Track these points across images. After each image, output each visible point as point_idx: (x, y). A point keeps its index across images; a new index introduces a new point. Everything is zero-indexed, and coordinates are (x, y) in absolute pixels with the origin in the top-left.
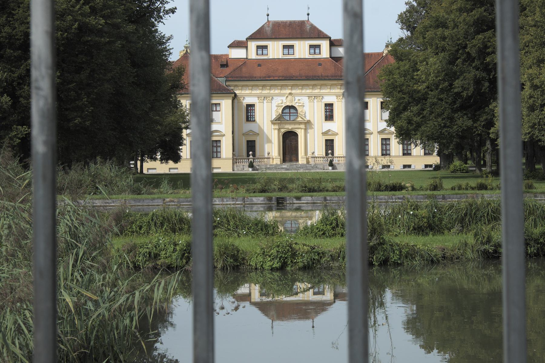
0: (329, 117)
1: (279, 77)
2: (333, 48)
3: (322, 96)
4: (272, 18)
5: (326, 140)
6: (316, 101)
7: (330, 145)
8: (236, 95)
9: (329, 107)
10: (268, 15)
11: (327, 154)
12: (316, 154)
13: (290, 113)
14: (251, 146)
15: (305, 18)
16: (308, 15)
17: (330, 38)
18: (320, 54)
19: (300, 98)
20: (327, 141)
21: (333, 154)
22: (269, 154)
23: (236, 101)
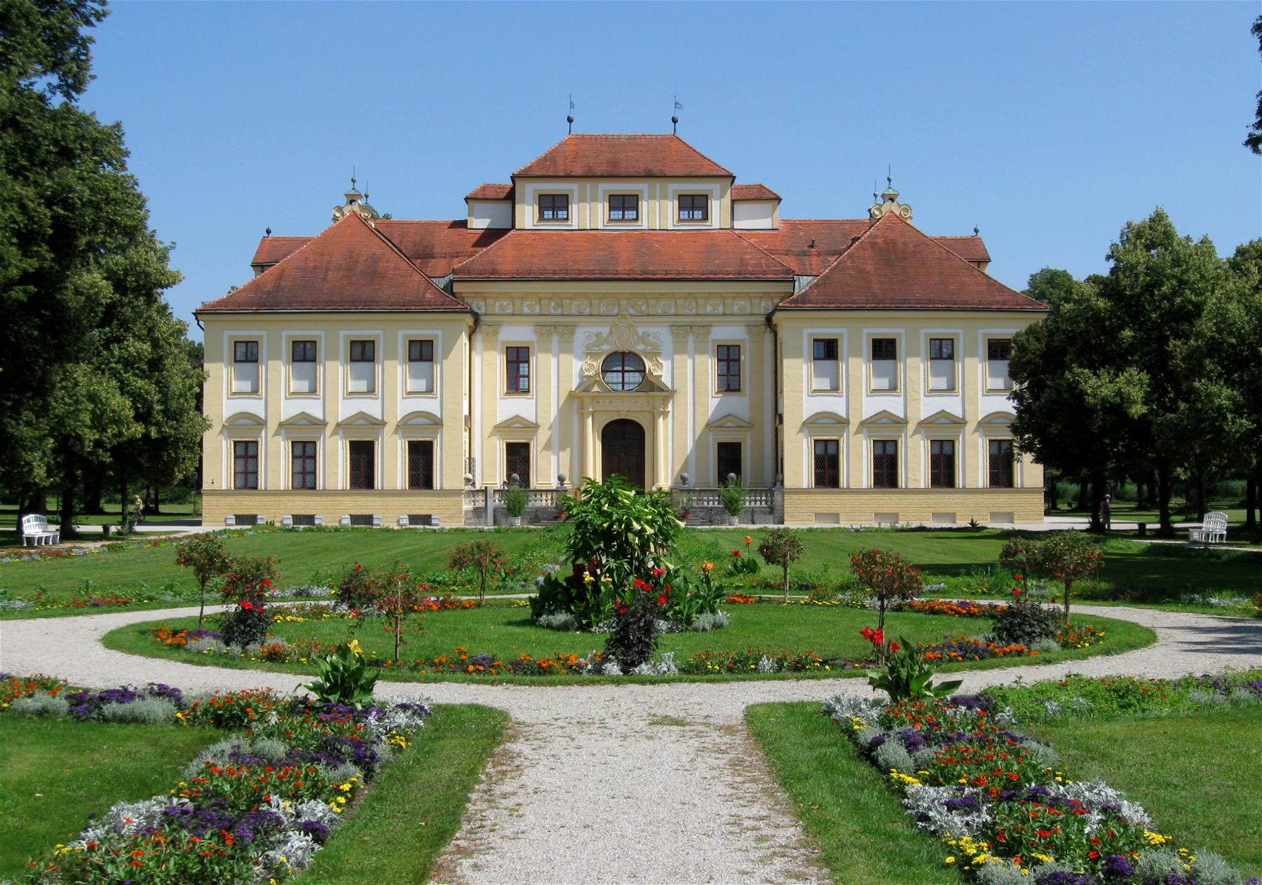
0: (730, 382)
1: (592, 272)
2: (738, 207)
3: (707, 327)
4: (579, 129)
5: (721, 446)
6: (691, 338)
7: (729, 457)
8: (476, 317)
9: (728, 357)
10: (570, 120)
11: (722, 478)
12: (691, 483)
13: (623, 372)
14: (518, 456)
15: (667, 129)
16: (675, 121)
17: (733, 178)
18: (705, 218)
19: (651, 330)
20: (721, 446)
21: (738, 484)
22: (561, 479)
23: (478, 338)
